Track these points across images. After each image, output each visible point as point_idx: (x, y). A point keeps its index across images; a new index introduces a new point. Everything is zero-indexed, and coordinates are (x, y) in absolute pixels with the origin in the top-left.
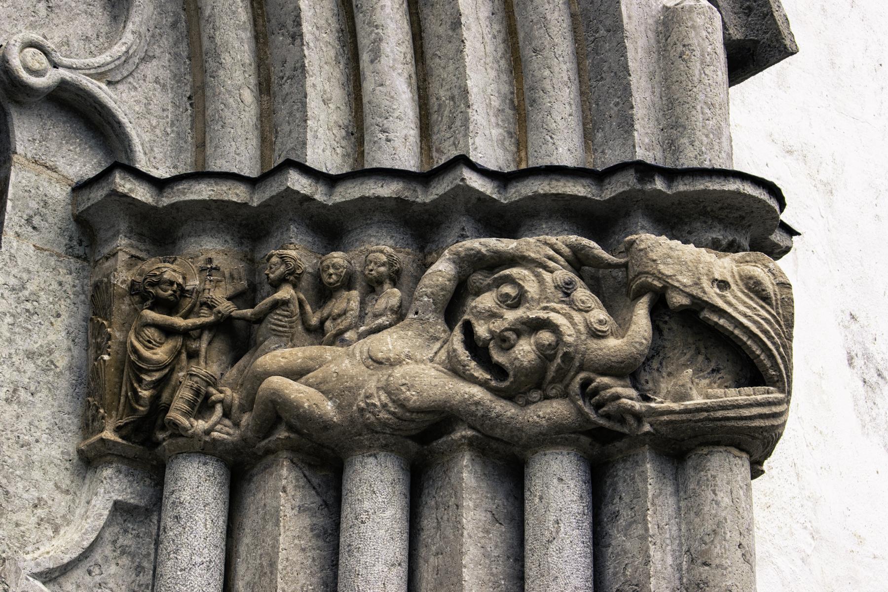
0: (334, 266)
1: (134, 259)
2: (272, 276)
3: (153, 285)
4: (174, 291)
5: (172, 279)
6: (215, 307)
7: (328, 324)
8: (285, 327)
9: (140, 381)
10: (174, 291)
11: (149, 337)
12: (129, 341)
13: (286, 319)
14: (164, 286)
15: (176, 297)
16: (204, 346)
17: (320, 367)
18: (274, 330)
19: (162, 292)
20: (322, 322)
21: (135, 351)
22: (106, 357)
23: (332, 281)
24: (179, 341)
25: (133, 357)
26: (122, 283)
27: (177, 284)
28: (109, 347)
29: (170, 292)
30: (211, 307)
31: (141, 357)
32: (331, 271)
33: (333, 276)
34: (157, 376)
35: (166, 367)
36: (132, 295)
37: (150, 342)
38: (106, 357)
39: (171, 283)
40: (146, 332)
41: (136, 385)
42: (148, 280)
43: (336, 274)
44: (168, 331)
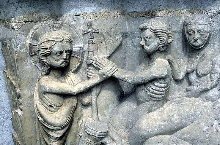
0: (199, 31)
1: (27, 24)
2: (147, 48)
3: (46, 56)
4: (64, 59)
5: (61, 50)
6: (100, 69)
7: (193, 77)
8: (163, 94)
9: (49, 136)
10: (64, 59)
11: (50, 103)
12: (35, 106)
13: (164, 89)
14: (55, 57)
15: (66, 62)
16: (94, 99)
17: (192, 123)
18: (153, 97)
19: (56, 62)
20: (187, 74)
21: (42, 116)
22: (20, 113)
23: (197, 44)
24: (74, 100)
25: (41, 119)
26: (21, 48)
27: (66, 52)
28: (21, 105)
29: (62, 60)
30: (97, 69)
31: (45, 120)
32: (197, 36)
33: (198, 41)
34: (60, 133)
35: (67, 125)
36: (32, 56)
37: (51, 106)
38: (20, 113)
39: (61, 53)
40: (47, 98)
41: (46, 139)
42: (41, 52)
43: (202, 39)
44: (65, 95)
